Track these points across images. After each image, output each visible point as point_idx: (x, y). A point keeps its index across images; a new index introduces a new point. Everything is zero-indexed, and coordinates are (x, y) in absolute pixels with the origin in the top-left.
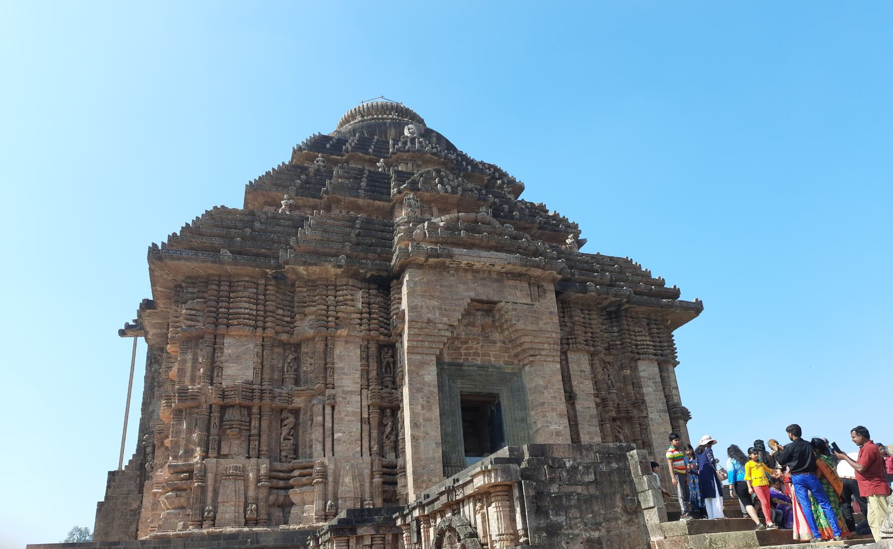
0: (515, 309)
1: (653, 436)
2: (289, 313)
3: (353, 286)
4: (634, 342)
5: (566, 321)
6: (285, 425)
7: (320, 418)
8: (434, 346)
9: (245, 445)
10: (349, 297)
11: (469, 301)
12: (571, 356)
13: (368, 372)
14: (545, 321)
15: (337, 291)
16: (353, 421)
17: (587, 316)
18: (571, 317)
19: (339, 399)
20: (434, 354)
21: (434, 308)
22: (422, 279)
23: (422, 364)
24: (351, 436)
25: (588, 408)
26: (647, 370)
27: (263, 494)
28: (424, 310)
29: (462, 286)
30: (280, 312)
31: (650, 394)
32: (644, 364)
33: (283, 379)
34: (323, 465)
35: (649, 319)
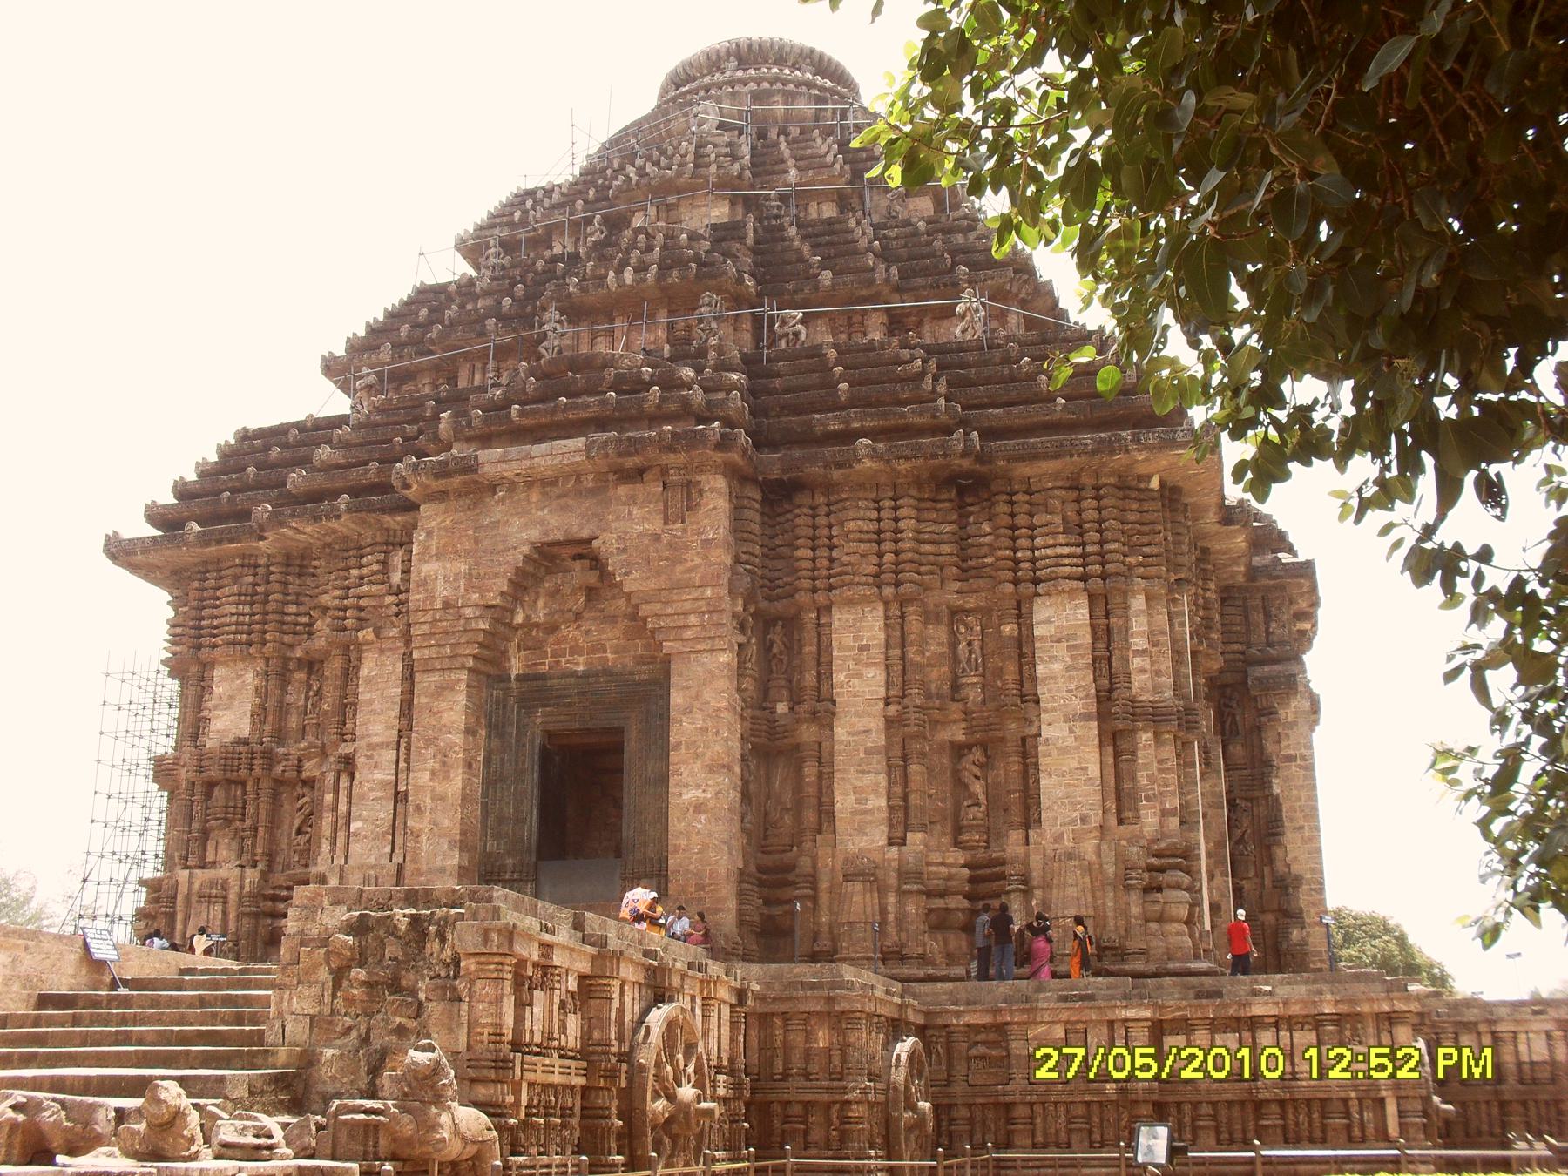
0: (624, 550)
1: (1042, 783)
3: (387, 544)
5: (834, 533)
6: (300, 809)
8: (460, 651)
9: (234, 846)
10: (375, 567)
11: (526, 549)
12: (841, 618)
14: (689, 565)
15: (362, 557)
16: (380, 798)
18: (841, 524)
19: (360, 760)
20: (463, 667)
21: (457, 575)
22: (444, 521)
24: (377, 826)
27: (246, 924)
28: (440, 581)
30: (292, 609)
31: (1054, 678)
32: (1051, 605)
33: (304, 727)
35: (1079, 488)
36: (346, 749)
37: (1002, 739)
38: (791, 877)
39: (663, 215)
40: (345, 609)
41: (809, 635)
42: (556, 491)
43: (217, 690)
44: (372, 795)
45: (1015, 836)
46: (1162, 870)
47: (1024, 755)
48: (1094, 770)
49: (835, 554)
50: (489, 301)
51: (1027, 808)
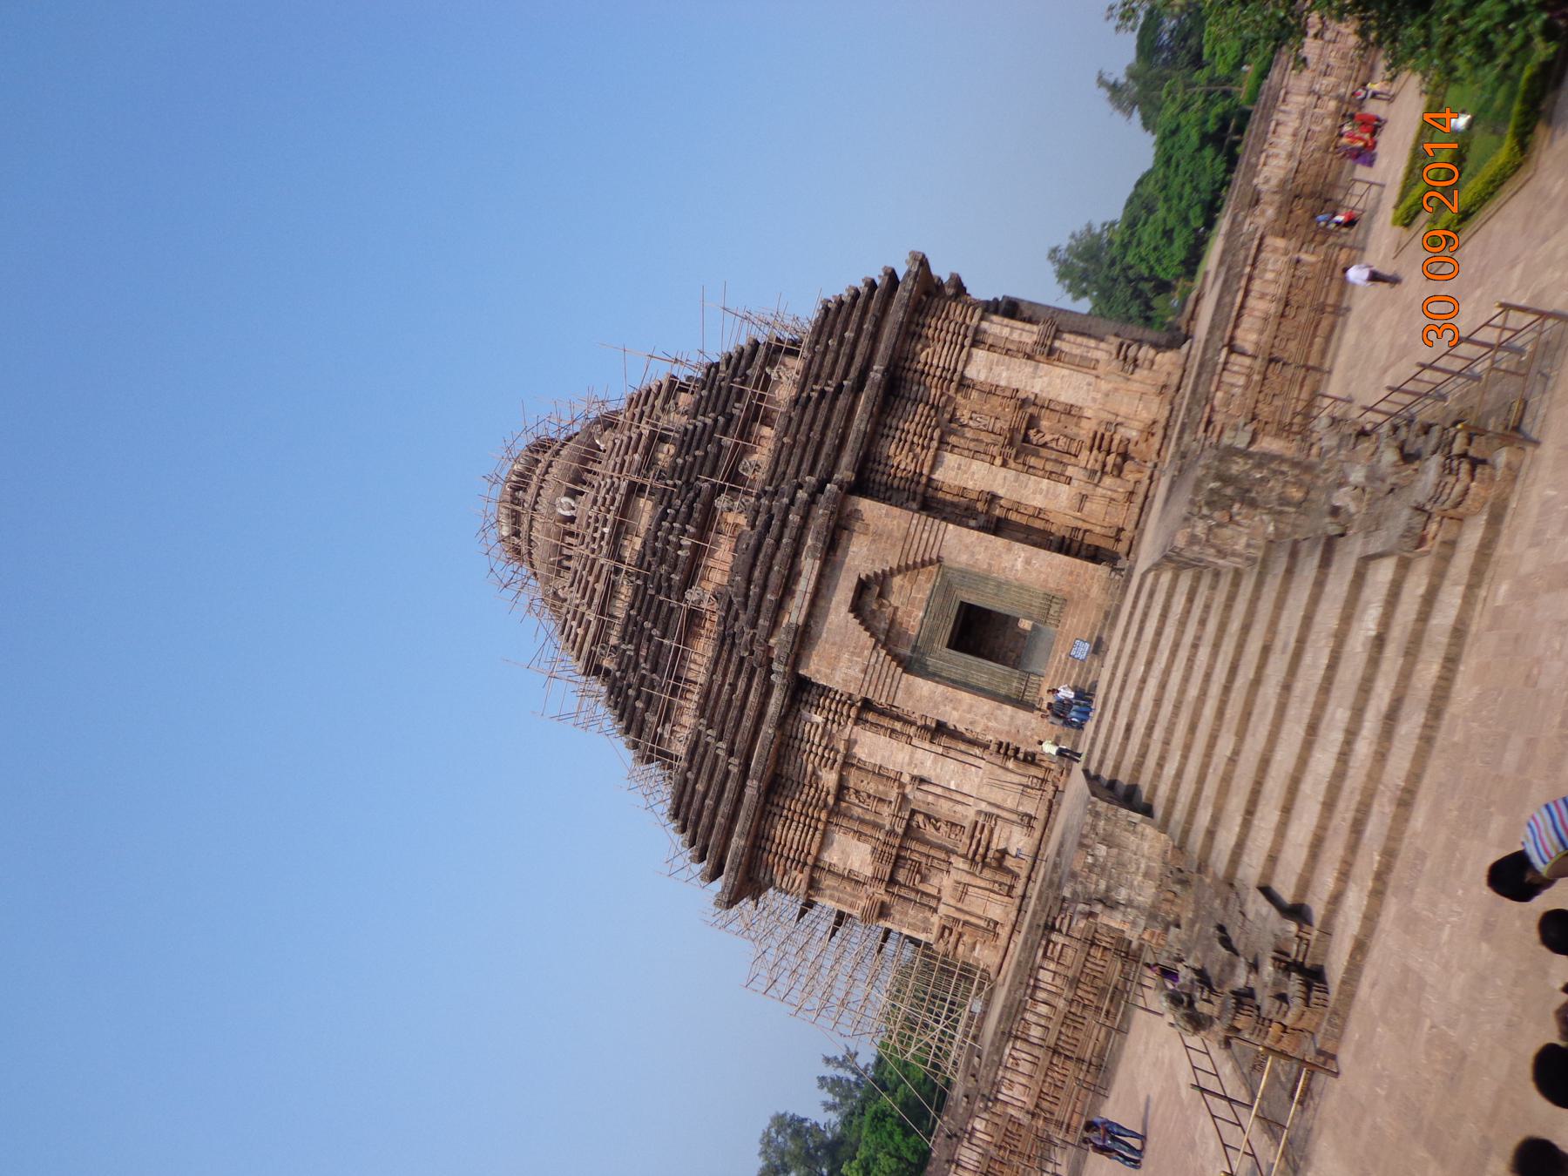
0: (873, 561)
1: (1062, 399)
2: (807, 788)
4: (938, 374)
7: (930, 798)
8: (891, 673)
9: (934, 871)
11: (851, 615)
13: (893, 731)
17: (892, 433)
18: (889, 457)
19: (915, 772)
23: (909, 692)
25: (1005, 478)
26: (980, 366)
27: (987, 873)
28: (851, 672)
29: (832, 617)
30: (804, 797)
34: (979, 812)
36: (906, 779)
37: (1032, 417)
38: (1068, 542)
39: (629, 537)
40: (823, 756)
41: (940, 495)
42: (824, 591)
43: (835, 860)
44: (938, 770)
45: (1084, 423)
46: (1125, 358)
47: (1042, 407)
48: (1065, 372)
49: (902, 467)
50: (645, 644)
51: (1069, 413)
